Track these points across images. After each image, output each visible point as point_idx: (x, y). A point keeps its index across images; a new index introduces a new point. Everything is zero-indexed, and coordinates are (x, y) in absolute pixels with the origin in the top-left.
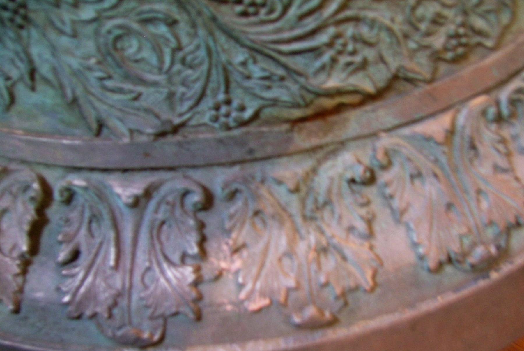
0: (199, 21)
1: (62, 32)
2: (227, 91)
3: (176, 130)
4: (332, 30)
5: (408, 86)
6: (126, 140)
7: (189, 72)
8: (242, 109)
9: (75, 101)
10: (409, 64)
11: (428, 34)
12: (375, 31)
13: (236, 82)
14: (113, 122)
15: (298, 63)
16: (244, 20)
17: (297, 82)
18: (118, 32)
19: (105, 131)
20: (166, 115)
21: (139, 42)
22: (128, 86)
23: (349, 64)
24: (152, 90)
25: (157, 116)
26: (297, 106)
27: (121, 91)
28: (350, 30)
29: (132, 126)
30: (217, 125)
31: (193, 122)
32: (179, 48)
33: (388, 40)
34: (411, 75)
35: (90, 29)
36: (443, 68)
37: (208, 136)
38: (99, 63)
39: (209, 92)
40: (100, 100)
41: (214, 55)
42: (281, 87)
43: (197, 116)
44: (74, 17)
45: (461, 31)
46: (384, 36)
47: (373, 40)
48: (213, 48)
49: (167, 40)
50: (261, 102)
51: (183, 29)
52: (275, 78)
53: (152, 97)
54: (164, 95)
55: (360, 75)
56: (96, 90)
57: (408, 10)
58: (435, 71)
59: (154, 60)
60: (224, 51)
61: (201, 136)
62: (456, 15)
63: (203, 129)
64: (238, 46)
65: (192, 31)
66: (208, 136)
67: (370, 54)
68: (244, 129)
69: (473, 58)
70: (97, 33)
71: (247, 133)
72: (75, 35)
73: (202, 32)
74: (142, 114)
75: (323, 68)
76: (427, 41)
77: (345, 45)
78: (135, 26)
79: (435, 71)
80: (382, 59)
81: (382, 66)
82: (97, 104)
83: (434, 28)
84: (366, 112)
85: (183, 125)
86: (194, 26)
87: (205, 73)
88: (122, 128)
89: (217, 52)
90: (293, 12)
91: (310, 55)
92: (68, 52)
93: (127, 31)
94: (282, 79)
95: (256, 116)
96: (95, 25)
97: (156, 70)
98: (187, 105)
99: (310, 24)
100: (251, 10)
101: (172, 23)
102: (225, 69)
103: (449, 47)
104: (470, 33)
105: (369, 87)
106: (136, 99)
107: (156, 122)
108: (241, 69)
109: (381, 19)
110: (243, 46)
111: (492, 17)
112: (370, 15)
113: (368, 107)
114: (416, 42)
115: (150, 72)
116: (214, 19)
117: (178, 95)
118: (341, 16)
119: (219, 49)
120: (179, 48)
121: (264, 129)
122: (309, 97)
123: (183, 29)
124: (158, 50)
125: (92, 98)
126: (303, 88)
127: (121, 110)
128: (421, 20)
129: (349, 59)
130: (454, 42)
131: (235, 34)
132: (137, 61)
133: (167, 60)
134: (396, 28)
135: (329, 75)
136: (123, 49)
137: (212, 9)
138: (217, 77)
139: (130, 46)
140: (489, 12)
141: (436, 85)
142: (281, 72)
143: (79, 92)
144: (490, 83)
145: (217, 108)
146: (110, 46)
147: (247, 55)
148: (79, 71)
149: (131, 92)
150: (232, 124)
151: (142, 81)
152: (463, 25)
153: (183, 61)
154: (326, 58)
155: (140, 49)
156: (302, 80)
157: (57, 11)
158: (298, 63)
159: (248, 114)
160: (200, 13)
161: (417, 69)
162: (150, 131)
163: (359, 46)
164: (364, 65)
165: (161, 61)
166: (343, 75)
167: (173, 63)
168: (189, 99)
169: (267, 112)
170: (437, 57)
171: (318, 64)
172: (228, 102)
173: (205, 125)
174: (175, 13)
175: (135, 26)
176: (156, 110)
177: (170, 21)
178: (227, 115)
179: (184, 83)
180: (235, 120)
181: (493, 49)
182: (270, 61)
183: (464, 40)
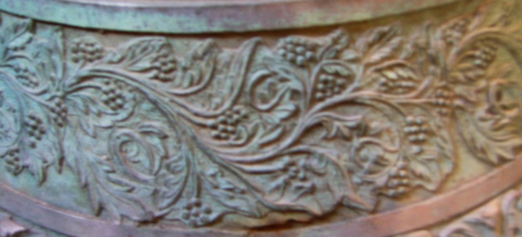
0: (184, 138)
1: (86, 133)
2: (199, 195)
3: (156, 220)
4: (286, 159)
5: (352, 214)
6: (117, 223)
7: (172, 176)
8: (209, 211)
9: (86, 186)
10: (350, 194)
11: (371, 172)
12: (323, 164)
13: (206, 189)
14: (111, 207)
15: (258, 181)
16: (218, 142)
17: (255, 197)
18: (125, 138)
19: (104, 213)
20: (150, 207)
21: (138, 148)
22: (125, 180)
23: (300, 188)
24: (142, 186)
25: (143, 208)
26: (252, 216)
27: (119, 183)
28: (302, 160)
29: (124, 212)
30: (187, 222)
31: (170, 217)
32: (166, 157)
33: (334, 173)
34: (354, 204)
35: (106, 133)
36: (385, 202)
37: (180, 230)
38: (108, 159)
39: (184, 194)
40: (104, 188)
41: (192, 166)
42: (241, 198)
43: (173, 212)
44: (97, 124)
45: (403, 173)
46: (331, 169)
47: (322, 171)
48: (192, 161)
49: (159, 150)
50: (224, 209)
51: (171, 143)
52: (237, 190)
53: (142, 192)
54: (151, 192)
55: (309, 198)
56: (103, 180)
57: (353, 150)
58: (377, 204)
59: (147, 163)
60: (199, 163)
61: (175, 229)
62: (398, 160)
63: (176, 223)
64: (211, 162)
65: (178, 145)
66: (180, 230)
67: (318, 181)
68: (208, 229)
69: (414, 198)
70: (110, 137)
71: (210, 232)
72: (95, 137)
73: (184, 147)
74: (132, 203)
75: (277, 188)
76: (370, 178)
77: (297, 172)
78: (137, 136)
79: (377, 204)
80: (328, 188)
81: (327, 193)
82: (101, 191)
83: (377, 168)
84: (314, 230)
85: (161, 217)
86: (179, 141)
87: (183, 179)
88: (116, 212)
89: (194, 164)
90: (256, 141)
91: (268, 176)
92: (88, 148)
93: (131, 139)
94: (243, 192)
95: (219, 220)
96: (109, 131)
97: (147, 171)
98: (167, 202)
99: (270, 151)
100: (223, 135)
101: (164, 137)
102: (199, 179)
103: (390, 184)
104: (411, 176)
105: (316, 209)
106: (130, 191)
107: (141, 212)
108: (211, 179)
109: (328, 155)
110: (215, 162)
111: (433, 165)
112: (320, 150)
113: (316, 227)
114: (360, 177)
115: (143, 172)
116: (194, 138)
117: (161, 193)
118: (295, 149)
119: (196, 162)
120: (166, 157)
121: (225, 231)
122: (264, 210)
123: (171, 143)
124: (151, 155)
125: (98, 185)
126: (259, 202)
127: (118, 199)
128: (365, 160)
129: (300, 184)
130: (395, 182)
131: (209, 152)
132: (135, 162)
133: (157, 164)
134: (342, 163)
135: (283, 195)
136: (126, 152)
137: (193, 131)
138: (192, 183)
139: (132, 151)
140: (430, 160)
141: (377, 216)
142: (243, 186)
143: (90, 179)
144: (431, 221)
145: (189, 208)
146: (118, 149)
147: (216, 170)
148: (93, 163)
149: (127, 185)
150: (199, 223)
151: (135, 178)
152: (404, 168)
153: (168, 167)
154: (280, 181)
155: (138, 154)
156: (259, 196)
157: (86, 117)
158: (258, 181)
159: (212, 217)
160: (184, 132)
161: (360, 200)
162: (136, 218)
163: (309, 174)
164: (312, 190)
165: (152, 164)
166: (295, 197)
167: (160, 167)
168: (169, 197)
169: (230, 218)
170: (379, 193)
171: (273, 184)
172: (198, 205)
173: (177, 220)
174: (167, 130)
175: (137, 136)
176: (144, 203)
177: (162, 136)
178: (196, 215)
179: (166, 184)
180: (202, 220)
181: (435, 192)
182: (235, 177)
183: (405, 181)
